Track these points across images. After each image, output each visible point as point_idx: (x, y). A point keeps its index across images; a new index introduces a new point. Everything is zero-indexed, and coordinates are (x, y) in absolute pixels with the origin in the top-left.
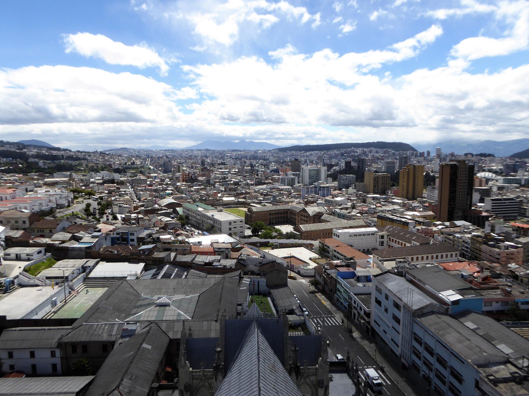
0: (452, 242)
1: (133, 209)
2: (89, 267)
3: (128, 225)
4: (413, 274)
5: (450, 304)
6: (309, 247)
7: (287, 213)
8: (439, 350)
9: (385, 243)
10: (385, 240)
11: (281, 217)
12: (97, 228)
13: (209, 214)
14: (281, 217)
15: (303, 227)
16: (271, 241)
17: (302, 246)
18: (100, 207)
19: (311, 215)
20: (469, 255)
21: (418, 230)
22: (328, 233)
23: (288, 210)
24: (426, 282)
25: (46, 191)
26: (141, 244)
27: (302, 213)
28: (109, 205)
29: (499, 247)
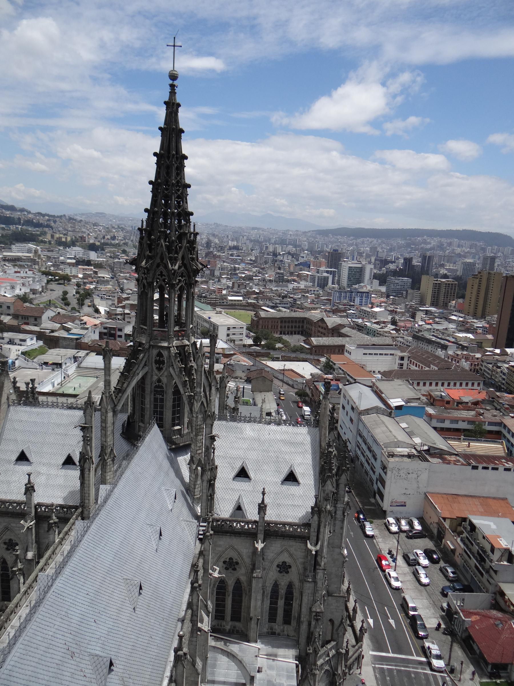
0: (490, 372)
2: (80, 357)
3: (113, 319)
4: (378, 385)
5: (394, 408)
6: (315, 363)
7: (303, 322)
8: (370, 441)
9: (405, 367)
10: (405, 362)
11: (295, 327)
12: (82, 320)
13: (206, 316)
14: (295, 327)
15: (315, 341)
16: (272, 353)
17: (306, 361)
18: (78, 296)
19: (330, 327)
20: (505, 388)
21: (458, 355)
22: (340, 349)
23: (305, 318)
24: (383, 391)
25: (16, 272)
26: (129, 341)
28: (88, 294)
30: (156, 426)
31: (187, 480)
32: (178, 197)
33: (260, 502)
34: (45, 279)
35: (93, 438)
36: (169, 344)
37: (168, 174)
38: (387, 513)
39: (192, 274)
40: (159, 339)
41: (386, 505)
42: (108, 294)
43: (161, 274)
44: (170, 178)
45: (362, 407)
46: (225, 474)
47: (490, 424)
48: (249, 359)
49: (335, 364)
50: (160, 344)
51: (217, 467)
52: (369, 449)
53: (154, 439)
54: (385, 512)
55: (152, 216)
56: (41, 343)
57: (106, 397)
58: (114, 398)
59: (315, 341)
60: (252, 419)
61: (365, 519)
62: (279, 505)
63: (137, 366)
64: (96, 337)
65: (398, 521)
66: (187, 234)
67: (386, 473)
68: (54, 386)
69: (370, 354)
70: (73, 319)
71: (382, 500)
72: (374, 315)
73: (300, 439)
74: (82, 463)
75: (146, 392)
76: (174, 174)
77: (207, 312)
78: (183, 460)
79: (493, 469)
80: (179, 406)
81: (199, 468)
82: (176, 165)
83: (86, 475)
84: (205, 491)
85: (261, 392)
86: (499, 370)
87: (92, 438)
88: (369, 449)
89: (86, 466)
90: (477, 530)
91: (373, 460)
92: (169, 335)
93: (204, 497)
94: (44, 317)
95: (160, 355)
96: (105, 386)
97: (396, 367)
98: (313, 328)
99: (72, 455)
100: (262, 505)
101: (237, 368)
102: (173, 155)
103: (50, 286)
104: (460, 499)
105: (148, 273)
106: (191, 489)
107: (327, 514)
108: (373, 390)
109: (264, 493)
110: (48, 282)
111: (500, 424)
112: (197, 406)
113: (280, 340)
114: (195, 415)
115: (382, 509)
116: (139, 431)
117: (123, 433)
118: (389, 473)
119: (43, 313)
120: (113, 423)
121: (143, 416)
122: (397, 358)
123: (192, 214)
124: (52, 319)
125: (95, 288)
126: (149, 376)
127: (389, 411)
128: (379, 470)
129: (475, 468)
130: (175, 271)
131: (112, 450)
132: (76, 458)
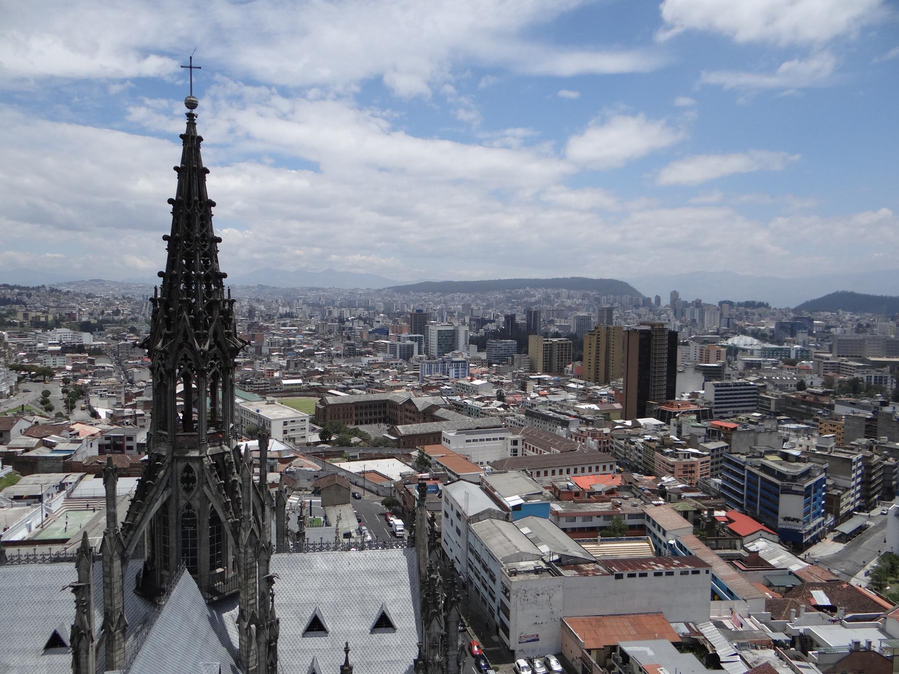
1: (123, 400)
6: (405, 459)
7: (385, 405)
8: (484, 557)
10: (520, 447)
11: (375, 413)
12: (73, 430)
13: (252, 409)
18: (66, 396)
19: (420, 410)
21: (582, 432)
24: (495, 487)
26: (143, 453)
27: (407, 406)
28: (82, 392)
29: (676, 456)
30: (186, 572)
31: (237, 645)
32: (205, 255)
33: (343, 664)
34: (14, 376)
35: (92, 602)
36: (201, 453)
37: (189, 225)
38: (516, 652)
39: (228, 355)
40: (186, 447)
41: (513, 643)
42: (111, 390)
43: (186, 359)
44: (192, 230)
45: (471, 513)
46: (290, 628)
47: (631, 516)
48: (316, 462)
49: (430, 458)
50: (187, 455)
51: (278, 622)
52: (485, 567)
53: (185, 593)
54: (513, 652)
55: (169, 281)
56: (9, 469)
57: (110, 538)
58: (122, 538)
59: (402, 429)
60: (325, 546)
61: (488, 666)
62: (369, 664)
63: (155, 489)
64: (95, 451)
65: (531, 662)
66: (219, 302)
67: (508, 598)
68: (30, 530)
69: (474, 440)
70: (58, 430)
71: (508, 636)
72: (475, 390)
73: (391, 565)
74: (76, 640)
75: (170, 524)
76: (198, 224)
77: (255, 403)
78: (230, 617)
79: (641, 575)
80: (219, 538)
81: (253, 626)
82: (199, 215)
83: (82, 660)
84: (262, 659)
85: (335, 505)
86: (633, 446)
87: (89, 602)
88: (485, 567)
89: (82, 645)
90: (631, 661)
91: (490, 583)
92: (199, 441)
93: (263, 668)
94: (14, 431)
95: (188, 469)
96: (108, 522)
97: (509, 454)
98: (399, 413)
99: (59, 631)
100: (346, 668)
101: (300, 476)
102: (196, 201)
103: (22, 386)
104: (606, 621)
105: (166, 358)
106: (243, 659)
107: (436, 668)
108: (481, 488)
109: (347, 650)
110: (20, 380)
111: (643, 515)
112: (245, 536)
113: (356, 433)
114: (242, 550)
115: (508, 648)
116: (162, 582)
117: (137, 588)
118: (513, 597)
119: (12, 425)
120: (123, 576)
121: (166, 560)
122: (509, 442)
123: (225, 276)
124: (27, 433)
125: (91, 383)
126: (174, 501)
127: (505, 513)
128: (499, 595)
129: (619, 577)
130: (205, 352)
131: (122, 616)
132: (66, 636)
